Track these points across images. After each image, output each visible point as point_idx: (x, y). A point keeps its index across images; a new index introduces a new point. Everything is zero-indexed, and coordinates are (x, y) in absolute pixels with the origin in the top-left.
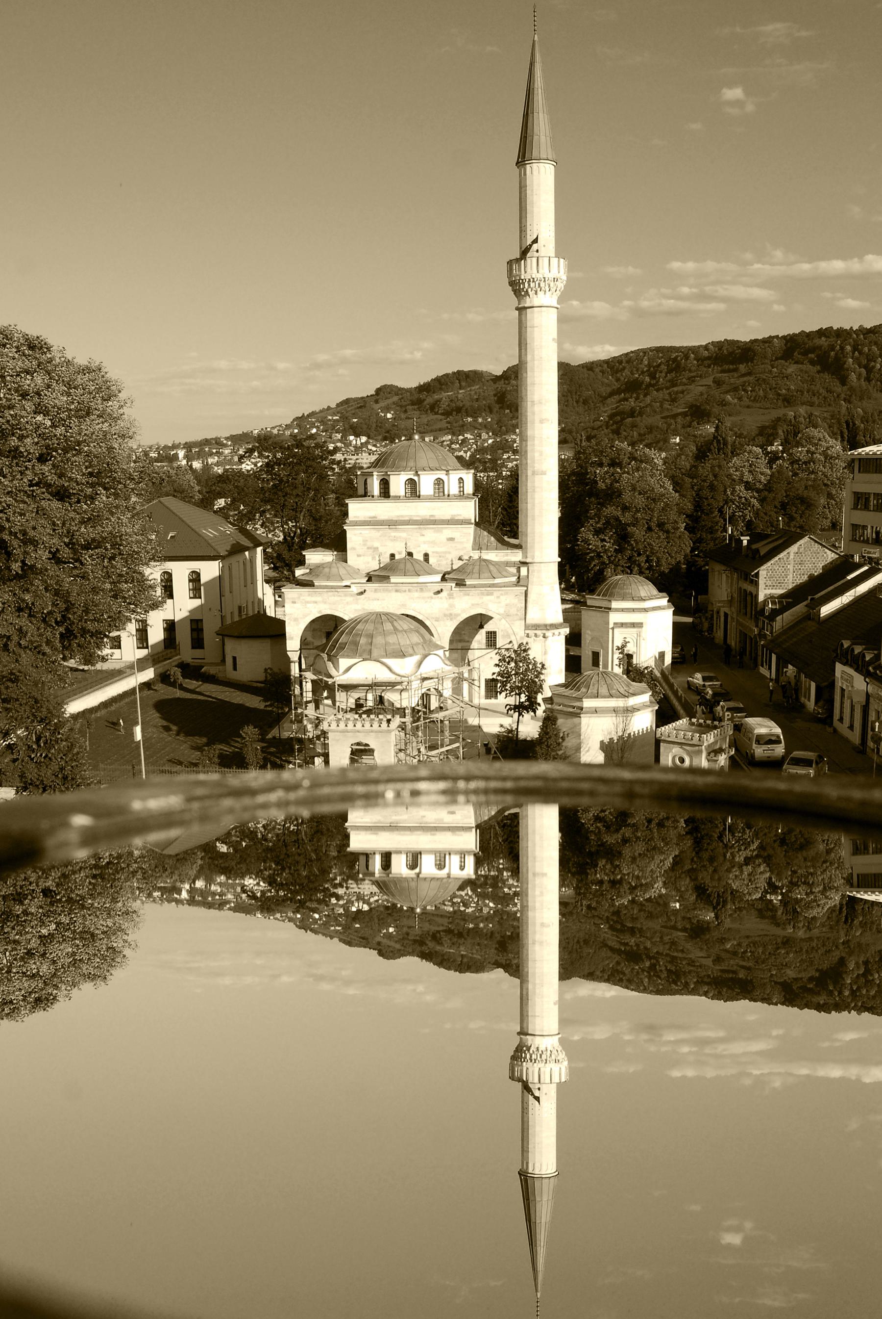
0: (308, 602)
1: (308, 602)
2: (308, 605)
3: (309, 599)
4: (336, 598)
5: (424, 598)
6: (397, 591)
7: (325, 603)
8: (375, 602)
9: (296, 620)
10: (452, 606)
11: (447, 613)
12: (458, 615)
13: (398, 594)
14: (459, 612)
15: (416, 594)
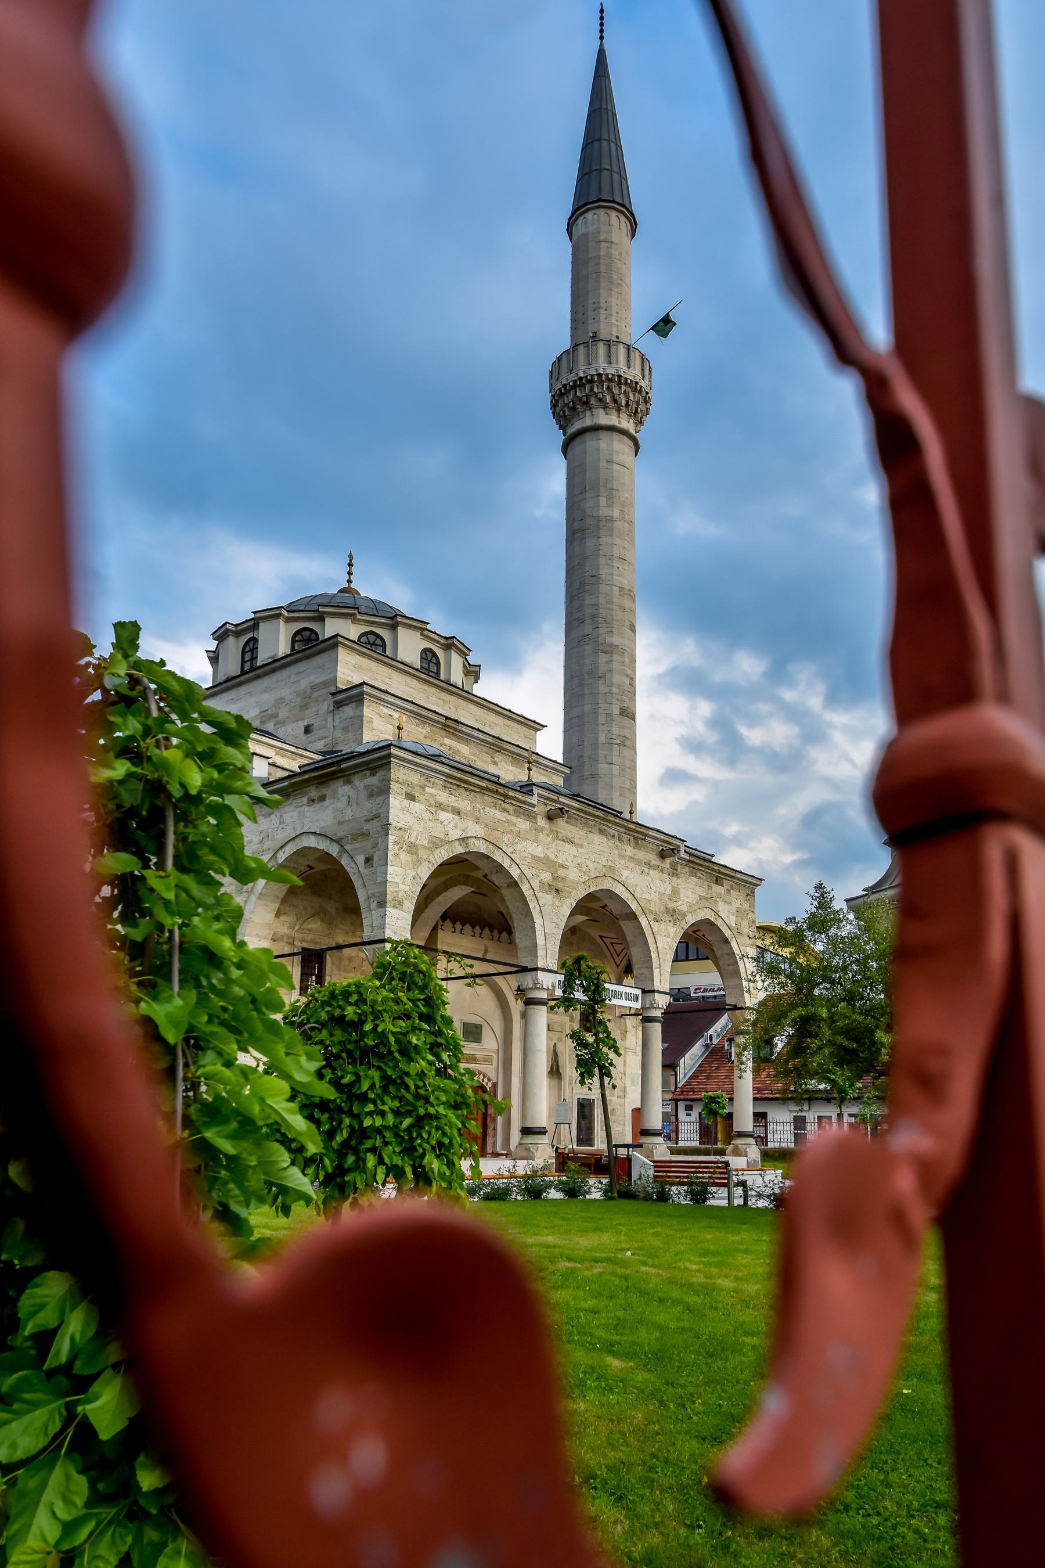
0: (440, 806)
1: (440, 806)
2: (444, 816)
3: (443, 797)
4: (499, 815)
5: (638, 862)
6: (602, 832)
7: (477, 820)
8: (568, 846)
9: (413, 849)
10: (675, 892)
11: (671, 905)
12: (684, 915)
13: (604, 839)
14: (684, 908)
15: (629, 850)
